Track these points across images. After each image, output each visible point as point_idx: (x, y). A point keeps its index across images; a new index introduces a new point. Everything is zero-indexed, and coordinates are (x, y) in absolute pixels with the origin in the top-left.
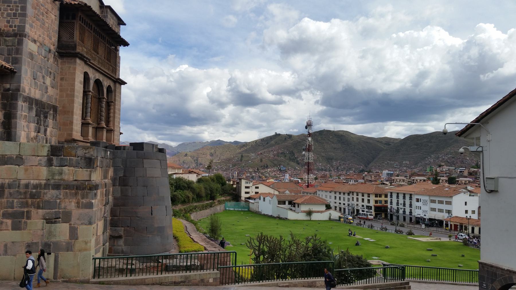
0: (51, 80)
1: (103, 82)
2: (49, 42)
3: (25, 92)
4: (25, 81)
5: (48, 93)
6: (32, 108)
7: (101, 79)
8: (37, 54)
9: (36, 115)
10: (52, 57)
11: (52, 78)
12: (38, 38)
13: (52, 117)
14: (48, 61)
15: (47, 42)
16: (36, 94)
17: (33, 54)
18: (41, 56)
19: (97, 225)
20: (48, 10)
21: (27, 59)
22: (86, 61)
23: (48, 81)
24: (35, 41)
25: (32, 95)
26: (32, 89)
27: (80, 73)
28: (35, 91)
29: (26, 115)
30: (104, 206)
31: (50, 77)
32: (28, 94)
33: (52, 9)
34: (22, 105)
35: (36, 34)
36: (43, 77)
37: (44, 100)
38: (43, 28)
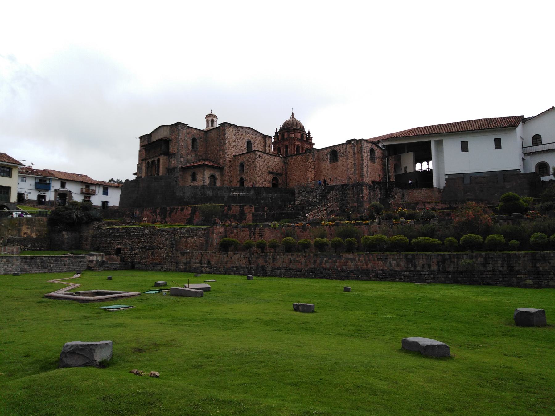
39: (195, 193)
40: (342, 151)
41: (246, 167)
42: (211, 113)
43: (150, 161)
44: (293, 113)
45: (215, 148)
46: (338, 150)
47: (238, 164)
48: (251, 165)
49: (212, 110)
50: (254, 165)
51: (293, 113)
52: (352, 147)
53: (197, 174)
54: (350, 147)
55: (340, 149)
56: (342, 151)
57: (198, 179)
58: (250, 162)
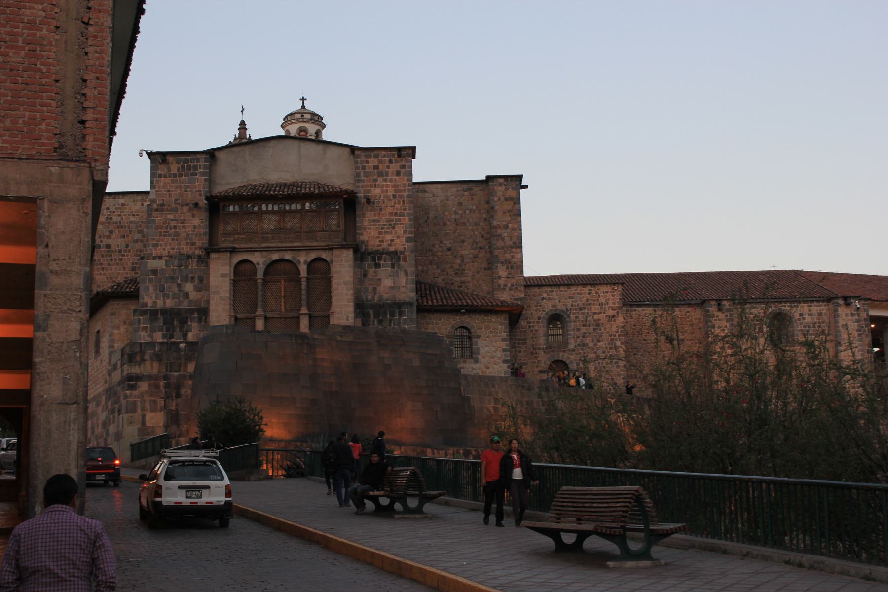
0: (194, 286)
1: (295, 259)
2: (191, 249)
3: (146, 305)
4: (145, 297)
5: (191, 299)
6: (157, 319)
7: (288, 256)
8: (164, 267)
9: (165, 323)
10: (195, 263)
11: (196, 281)
12: (169, 252)
13: (196, 320)
14: (187, 267)
15: (186, 249)
16: (169, 304)
17: (157, 270)
18: (172, 268)
19: (144, 416)
20: (185, 220)
21: (147, 277)
22: (233, 251)
23: (189, 287)
24: (160, 258)
25: (160, 305)
26: (158, 301)
27: (220, 267)
28: (164, 303)
29: (147, 327)
30: (162, 398)
31: (192, 282)
32: (152, 307)
33: (193, 215)
34: (139, 319)
35: (164, 249)
36: (179, 286)
37: (185, 305)
38: (177, 240)
39: (527, 402)
40: (808, 319)
41: (579, 329)
42: (303, 107)
43: (259, 260)
44: (243, 124)
45: (449, 249)
46: (797, 316)
47: (543, 314)
48: (598, 325)
49: (303, 99)
50: (614, 329)
51: (243, 124)
52: (852, 315)
53: (479, 337)
54: (847, 315)
55: (801, 315)
56: (808, 319)
57: (482, 351)
58: (596, 317)
